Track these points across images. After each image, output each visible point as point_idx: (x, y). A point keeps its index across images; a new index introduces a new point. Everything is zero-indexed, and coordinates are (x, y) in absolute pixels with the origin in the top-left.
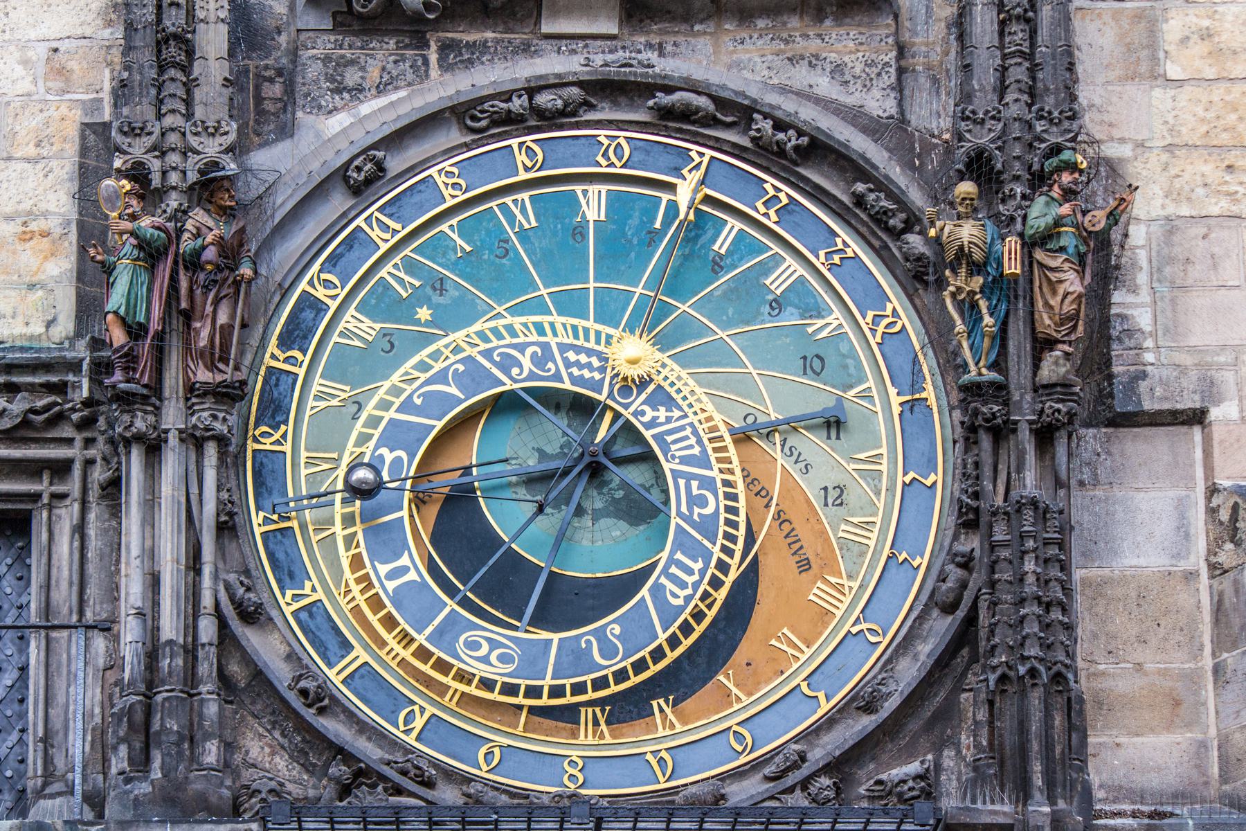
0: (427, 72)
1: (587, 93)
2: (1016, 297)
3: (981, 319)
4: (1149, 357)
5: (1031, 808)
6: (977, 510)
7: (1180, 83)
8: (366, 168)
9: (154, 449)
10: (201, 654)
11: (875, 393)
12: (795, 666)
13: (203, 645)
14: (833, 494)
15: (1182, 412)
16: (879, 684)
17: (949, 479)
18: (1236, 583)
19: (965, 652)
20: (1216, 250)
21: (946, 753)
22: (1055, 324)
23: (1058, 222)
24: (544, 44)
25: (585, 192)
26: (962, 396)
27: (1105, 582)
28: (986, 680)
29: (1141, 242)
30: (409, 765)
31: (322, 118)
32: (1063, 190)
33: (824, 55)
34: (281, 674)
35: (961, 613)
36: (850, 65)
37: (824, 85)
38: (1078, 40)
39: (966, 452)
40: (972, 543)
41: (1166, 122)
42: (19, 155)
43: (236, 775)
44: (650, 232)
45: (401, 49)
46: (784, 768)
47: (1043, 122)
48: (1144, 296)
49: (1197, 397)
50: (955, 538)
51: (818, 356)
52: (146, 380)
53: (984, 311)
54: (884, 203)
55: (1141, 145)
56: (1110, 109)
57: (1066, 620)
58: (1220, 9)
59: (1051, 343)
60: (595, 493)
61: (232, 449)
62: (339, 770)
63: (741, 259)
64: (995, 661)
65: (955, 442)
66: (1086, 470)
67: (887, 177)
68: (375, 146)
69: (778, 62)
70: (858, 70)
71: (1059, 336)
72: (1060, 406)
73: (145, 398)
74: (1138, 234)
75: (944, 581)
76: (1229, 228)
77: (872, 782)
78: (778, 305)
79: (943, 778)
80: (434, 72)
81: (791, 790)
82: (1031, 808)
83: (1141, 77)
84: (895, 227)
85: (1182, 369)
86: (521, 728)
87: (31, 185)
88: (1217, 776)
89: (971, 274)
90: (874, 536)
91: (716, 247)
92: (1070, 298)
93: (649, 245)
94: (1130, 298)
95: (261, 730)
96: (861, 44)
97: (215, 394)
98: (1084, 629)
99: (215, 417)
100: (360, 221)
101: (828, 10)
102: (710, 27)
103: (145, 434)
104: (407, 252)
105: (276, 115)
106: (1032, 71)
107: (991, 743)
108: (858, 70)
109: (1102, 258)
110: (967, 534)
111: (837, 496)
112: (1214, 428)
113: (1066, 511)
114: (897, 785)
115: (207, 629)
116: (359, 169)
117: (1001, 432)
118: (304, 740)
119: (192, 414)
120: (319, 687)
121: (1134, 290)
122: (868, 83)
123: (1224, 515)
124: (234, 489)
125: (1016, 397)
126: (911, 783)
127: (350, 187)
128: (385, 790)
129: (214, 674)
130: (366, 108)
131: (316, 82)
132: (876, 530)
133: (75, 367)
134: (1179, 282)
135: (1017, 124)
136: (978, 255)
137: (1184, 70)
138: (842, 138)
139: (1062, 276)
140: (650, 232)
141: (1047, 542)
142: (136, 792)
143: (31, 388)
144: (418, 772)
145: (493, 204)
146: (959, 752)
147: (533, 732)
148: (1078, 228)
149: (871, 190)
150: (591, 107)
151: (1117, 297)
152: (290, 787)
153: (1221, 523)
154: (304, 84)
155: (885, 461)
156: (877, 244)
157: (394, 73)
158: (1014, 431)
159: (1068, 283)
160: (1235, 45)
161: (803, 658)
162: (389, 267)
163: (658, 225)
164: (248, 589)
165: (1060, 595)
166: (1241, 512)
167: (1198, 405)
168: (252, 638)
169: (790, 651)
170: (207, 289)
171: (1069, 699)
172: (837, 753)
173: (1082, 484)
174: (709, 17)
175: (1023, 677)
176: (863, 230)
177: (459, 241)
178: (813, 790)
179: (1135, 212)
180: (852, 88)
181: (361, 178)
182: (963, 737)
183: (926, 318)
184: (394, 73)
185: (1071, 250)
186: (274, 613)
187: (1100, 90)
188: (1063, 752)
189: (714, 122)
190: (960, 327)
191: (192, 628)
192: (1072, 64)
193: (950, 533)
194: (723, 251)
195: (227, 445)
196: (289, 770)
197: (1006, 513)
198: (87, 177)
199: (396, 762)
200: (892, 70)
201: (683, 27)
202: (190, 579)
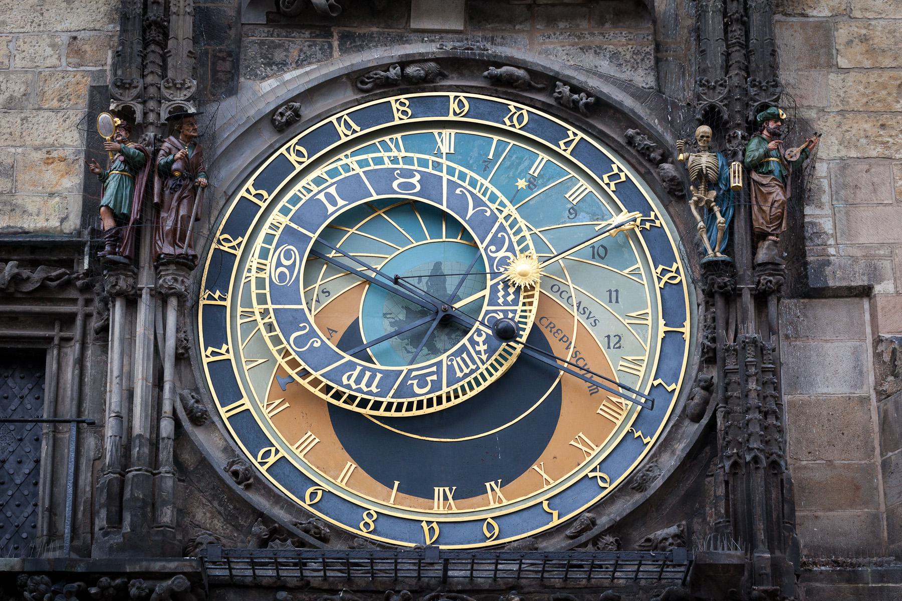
0: (331, 53)
1: (442, 67)
2: (739, 205)
3: (716, 218)
4: (832, 251)
5: (756, 555)
6: (714, 350)
7: (847, 70)
8: (287, 114)
9: (132, 302)
12: (588, 459)
13: (163, 439)
14: (613, 341)
15: (855, 288)
16: (648, 470)
17: (695, 330)
18: (896, 402)
19: (708, 449)
20: (875, 180)
21: (695, 520)
22: (767, 222)
23: (767, 154)
24: (413, 36)
25: (440, 134)
26: (703, 271)
27: (804, 404)
28: (723, 467)
29: (824, 174)
30: (311, 526)
31: (258, 82)
32: (770, 133)
33: (605, 47)
34: (219, 461)
35: (704, 421)
36: (623, 53)
38: (778, 42)
39: (707, 310)
41: (839, 96)
43: (185, 532)
44: (485, 161)
45: (313, 37)
46: (580, 531)
47: (755, 89)
49: (865, 278)
50: (700, 369)
51: (602, 246)
55: (822, 110)
56: (800, 87)
57: (779, 424)
58: (873, 23)
59: (764, 236)
60: (446, 338)
61: (189, 304)
62: (259, 529)
63: (549, 180)
64: (729, 452)
65: (698, 305)
66: (790, 327)
67: (649, 125)
68: (294, 99)
69: (573, 50)
71: (770, 230)
72: (771, 278)
73: (125, 266)
74: (822, 169)
75: (692, 399)
76: (884, 165)
77: (643, 540)
78: (574, 211)
79: (694, 537)
80: (336, 54)
81: (585, 545)
82: (756, 555)
83: (821, 66)
84: (655, 159)
85: (855, 259)
86: (392, 501)
88: (886, 539)
89: (707, 190)
90: (643, 369)
91: (531, 172)
92: (776, 205)
93: (485, 170)
94: (818, 212)
95: (204, 501)
96: (630, 40)
97: (178, 264)
98: (791, 436)
99: (176, 280)
100: (283, 150)
101: (608, 17)
102: (527, 26)
103: (126, 291)
105: (227, 82)
106: (747, 56)
107: (727, 511)
108: (628, 57)
109: (797, 179)
110: (708, 367)
111: (616, 342)
112: (878, 299)
113: (777, 349)
114: (661, 541)
115: (167, 427)
116: (282, 114)
117: (731, 297)
118: (235, 508)
119: (160, 278)
120: (246, 469)
121: (820, 206)
122: (636, 66)
123: (887, 357)
124: (189, 332)
126: (670, 540)
127: (276, 127)
128: (293, 543)
129: (171, 459)
130: (288, 76)
131: (254, 58)
132: (644, 365)
134: (850, 201)
135: (737, 90)
136: (712, 175)
137: (850, 62)
138: (618, 99)
139: (770, 189)
140: (485, 161)
141: (764, 371)
142: (111, 542)
144: (316, 530)
145: (376, 141)
146: (704, 519)
147: (400, 504)
148: (781, 160)
149: (638, 134)
150: (444, 77)
151: (808, 210)
152: (224, 541)
153: (884, 363)
154: (245, 60)
155: (650, 318)
156: (643, 170)
157: (309, 53)
158: (740, 295)
159: (775, 195)
160: (884, 46)
161: (593, 454)
163: (491, 157)
164: (197, 402)
165: (774, 407)
166: (898, 354)
169: (584, 449)
170: (173, 190)
171: (782, 480)
172: (618, 519)
173: (787, 337)
175: (749, 462)
176: (633, 161)
178: (600, 545)
179: (819, 154)
180: (624, 69)
181: (284, 121)
182: (708, 509)
183: (677, 221)
184: (309, 53)
185: (777, 173)
186: (216, 419)
187: (793, 74)
188: (778, 516)
189: (530, 88)
190: (701, 224)
192: (774, 51)
193: (696, 367)
194: (536, 175)
195: (185, 301)
196: (223, 529)
197: (735, 350)
198: (91, 119)
199: (301, 524)
200: (652, 57)
201: (509, 26)
202: (156, 394)
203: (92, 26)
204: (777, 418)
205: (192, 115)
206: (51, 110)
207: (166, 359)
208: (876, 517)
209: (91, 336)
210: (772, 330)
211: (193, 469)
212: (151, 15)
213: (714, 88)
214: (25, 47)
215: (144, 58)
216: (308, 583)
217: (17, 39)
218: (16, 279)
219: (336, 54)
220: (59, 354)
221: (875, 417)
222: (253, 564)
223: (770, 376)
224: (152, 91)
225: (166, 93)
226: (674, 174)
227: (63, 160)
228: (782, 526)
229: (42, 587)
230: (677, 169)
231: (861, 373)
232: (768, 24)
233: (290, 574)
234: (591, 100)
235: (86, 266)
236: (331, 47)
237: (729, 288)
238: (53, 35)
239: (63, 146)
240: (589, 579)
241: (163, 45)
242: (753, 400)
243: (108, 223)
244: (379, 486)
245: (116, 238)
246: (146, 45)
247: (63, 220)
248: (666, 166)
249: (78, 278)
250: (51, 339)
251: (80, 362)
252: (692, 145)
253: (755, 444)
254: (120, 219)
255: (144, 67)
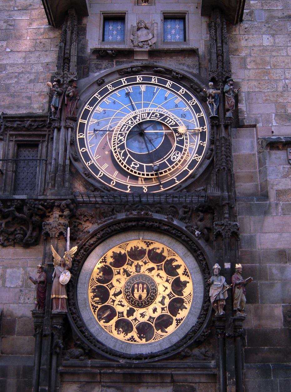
4: (246, 116)
6: (213, 141)
7: (250, 69)
10: (66, 167)
11: (195, 121)
15: (252, 125)
19: (212, 167)
20: (257, 97)
24: (135, 61)
25: (142, 86)
34: (81, 171)
35: (211, 159)
37: (185, 68)
40: (213, 147)
42: (40, 81)
48: (244, 105)
49: (255, 122)
50: (210, 146)
52: (58, 117)
53: (214, 105)
54: (196, 87)
61: (74, 130)
64: (217, 167)
68: (103, 77)
70: (192, 66)
74: (243, 95)
80: (115, 66)
87: (42, 87)
94: (242, 105)
98: (234, 163)
99: (70, 123)
102: (165, 58)
104: (109, 96)
106: (223, 64)
108: (192, 66)
115: (68, 162)
116: (100, 81)
118: (86, 183)
121: (243, 104)
123: (260, 143)
125: (221, 120)
128: (101, 192)
130: (102, 72)
133: (47, 117)
143: (38, 121)
145: (125, 88)
146: (211, 185)
150: (143, 71)
151: (239, 105)
158: (220, 126)
160: (260, 63)
161: (181, 169)
162: (105, 99)
164: (76, 155)
167: (255, 124)
168: (76, 164)
170: (70, 100)
171: (231, 174)
174: (165, 57)
177: (118, 95)
178: (182, 192)
181: (101, 82)
189: (165, 73)
191: (64, 162)
202: (65, 153)
203: (52, 61)
204: (230, 158)
205: (76, 81)
206: (41, 82)
207: (68, 144)
208: (257, 185)
209: (50, 139)
210: (229, 136)
211: (75, 173)
212: (66, 56)
213: (214, 72)
214: (35, 67)
215: (64, 67)
216: (104, 202)
217: (33, 65)
218: (30, 125)
219: (115, 66)
220: (42, 145)
221: (257, 159)
222: (89, 197)
223: (228, 147)
224: (65, 75)
225: (69, 76)
226: (204, 95)
227: (43, 95)
228: (231, 186)
229: (32, 203)
230: (204, 94)
231: (253, 147)
232: (228, 55)
233: (99, 200)
234: (181, 76)
235: (49, 121)
236: (113, 64)
237: (217, 124)
238: (42, 64)
239: (44, 92)
240: (179, 201)
241: (69, 64)
242: (224, 153)
243: (53, 109)
244: (124, 177)
245: (55, 113)
246: (64, 64)
247: (43, 110)
248: (201, 93)
249: (47, 125)
250: (40, 141)
251: (47, 147)
252: (208, 88)
253: (224, 164)
254: (56, 108)
255: (63, 69)
